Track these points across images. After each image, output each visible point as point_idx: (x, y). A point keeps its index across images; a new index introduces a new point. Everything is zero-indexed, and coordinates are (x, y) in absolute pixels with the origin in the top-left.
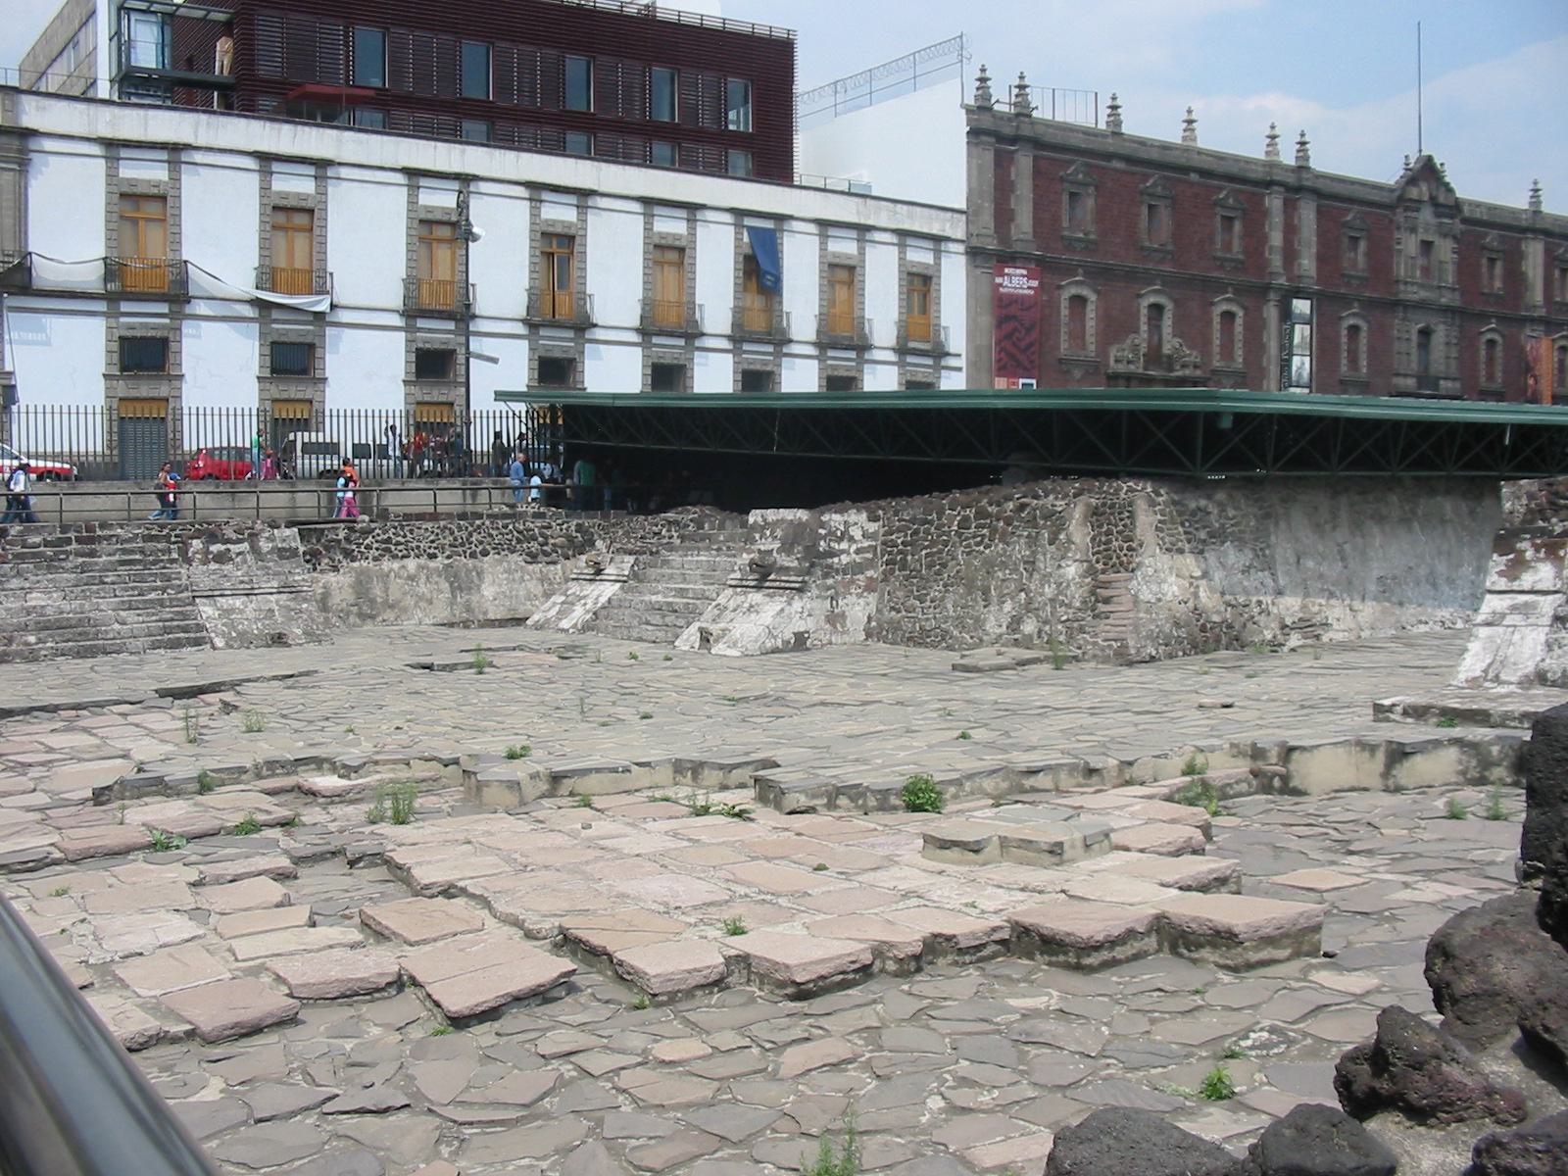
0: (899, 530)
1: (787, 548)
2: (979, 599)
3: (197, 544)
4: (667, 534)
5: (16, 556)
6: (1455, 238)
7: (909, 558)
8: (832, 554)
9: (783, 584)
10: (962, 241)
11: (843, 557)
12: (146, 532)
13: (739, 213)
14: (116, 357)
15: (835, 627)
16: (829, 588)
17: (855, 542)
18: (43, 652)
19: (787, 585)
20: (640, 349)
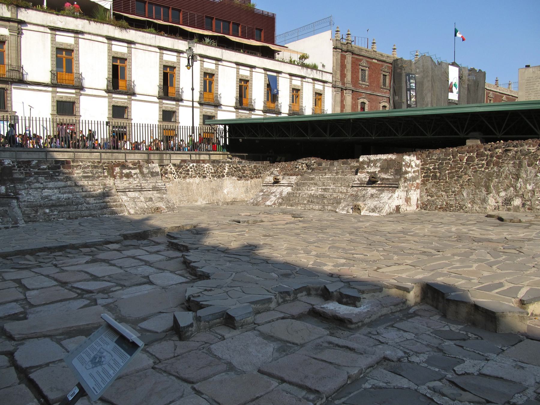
1: (384, 169)
2: (483, 191)
3: (117, 169)
5: (36, 173)
7: (438, 174)
8: (407, 172)
9: (387, 185)
10: (331, 83)
11: (410, 174)
12: (92, 164)
13: (265, 69)
14: (55, 108)
15: (408, 204)
16: (406, 187)
17: (413, 168)
18: (53, 217)
20: (235, 114)
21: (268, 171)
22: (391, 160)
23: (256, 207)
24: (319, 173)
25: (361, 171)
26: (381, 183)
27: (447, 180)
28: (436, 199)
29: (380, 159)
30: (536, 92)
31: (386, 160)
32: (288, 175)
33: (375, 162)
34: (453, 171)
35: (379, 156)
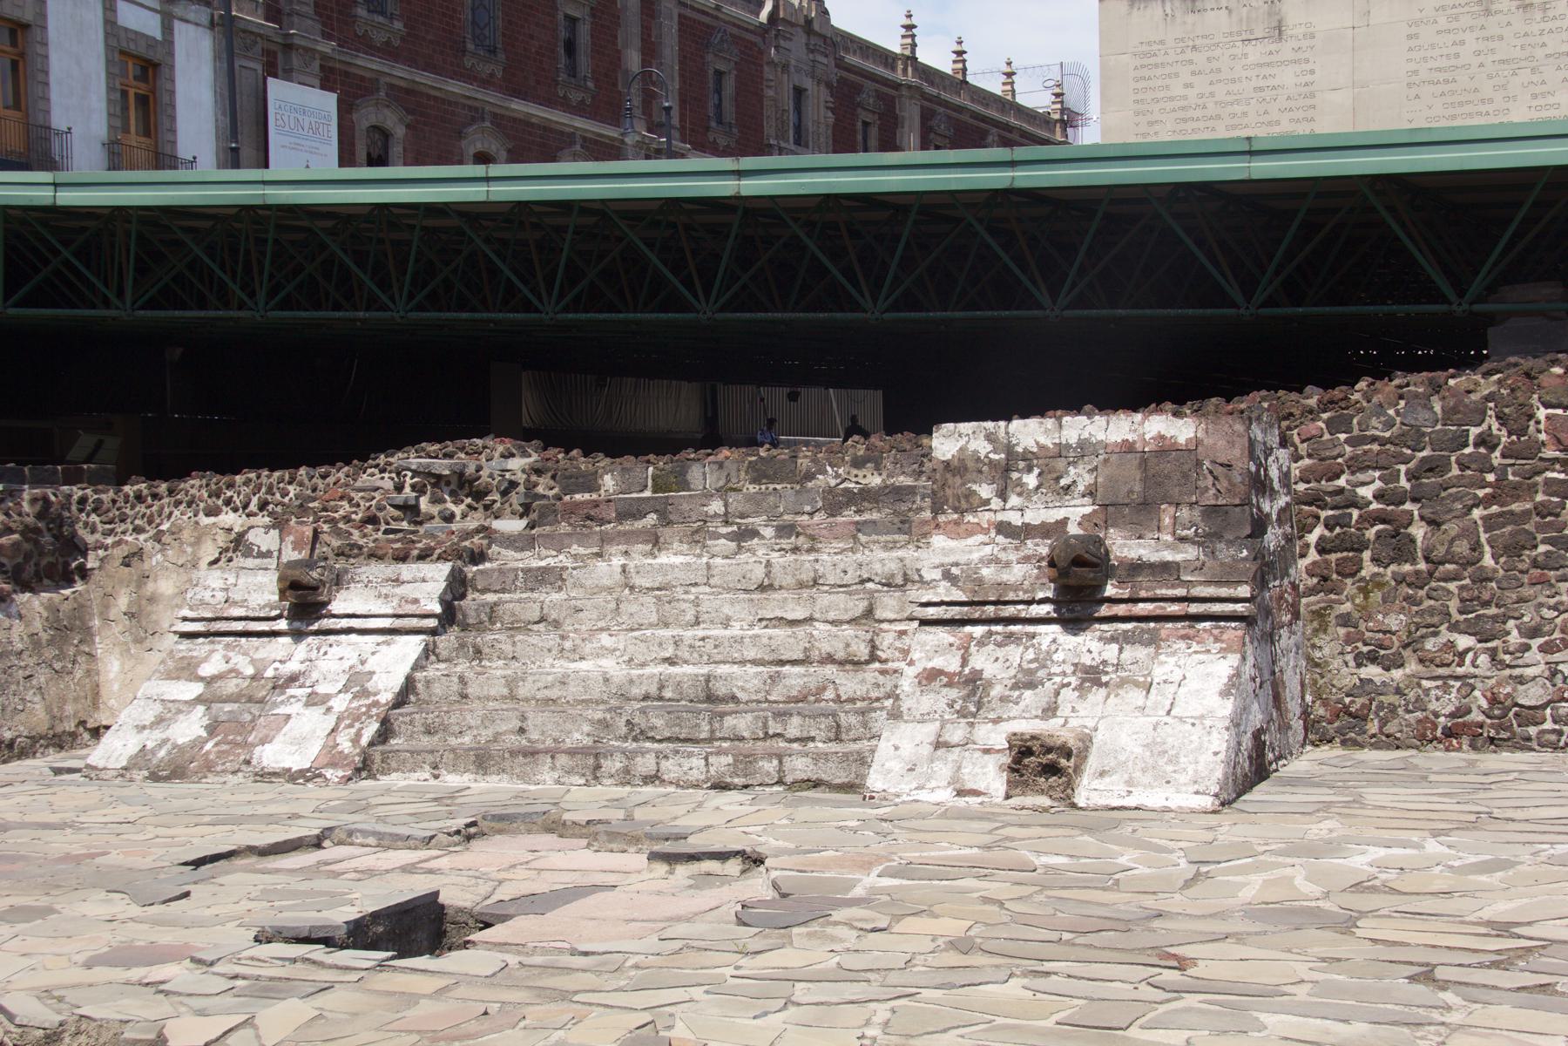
0: (1356, 465)
4: (435, 510)
6: (829, 85)
7: (1418, 531)
9: (1174, 608)
19: (1194, 609)
21: (138, 530)
22: (1166, 448)
23: (177, 787)
24: (605, 540)
25: (957, 523)
26: (1126, 593)
27: (1488, 561)
28: (1415, 680)
29: (1085, 449)
30: (1181, 114)
31: (1128, 448)
32: (375, 556)
33: (1051, 462)
34: (1516, 507)
35: (1078, 427)
